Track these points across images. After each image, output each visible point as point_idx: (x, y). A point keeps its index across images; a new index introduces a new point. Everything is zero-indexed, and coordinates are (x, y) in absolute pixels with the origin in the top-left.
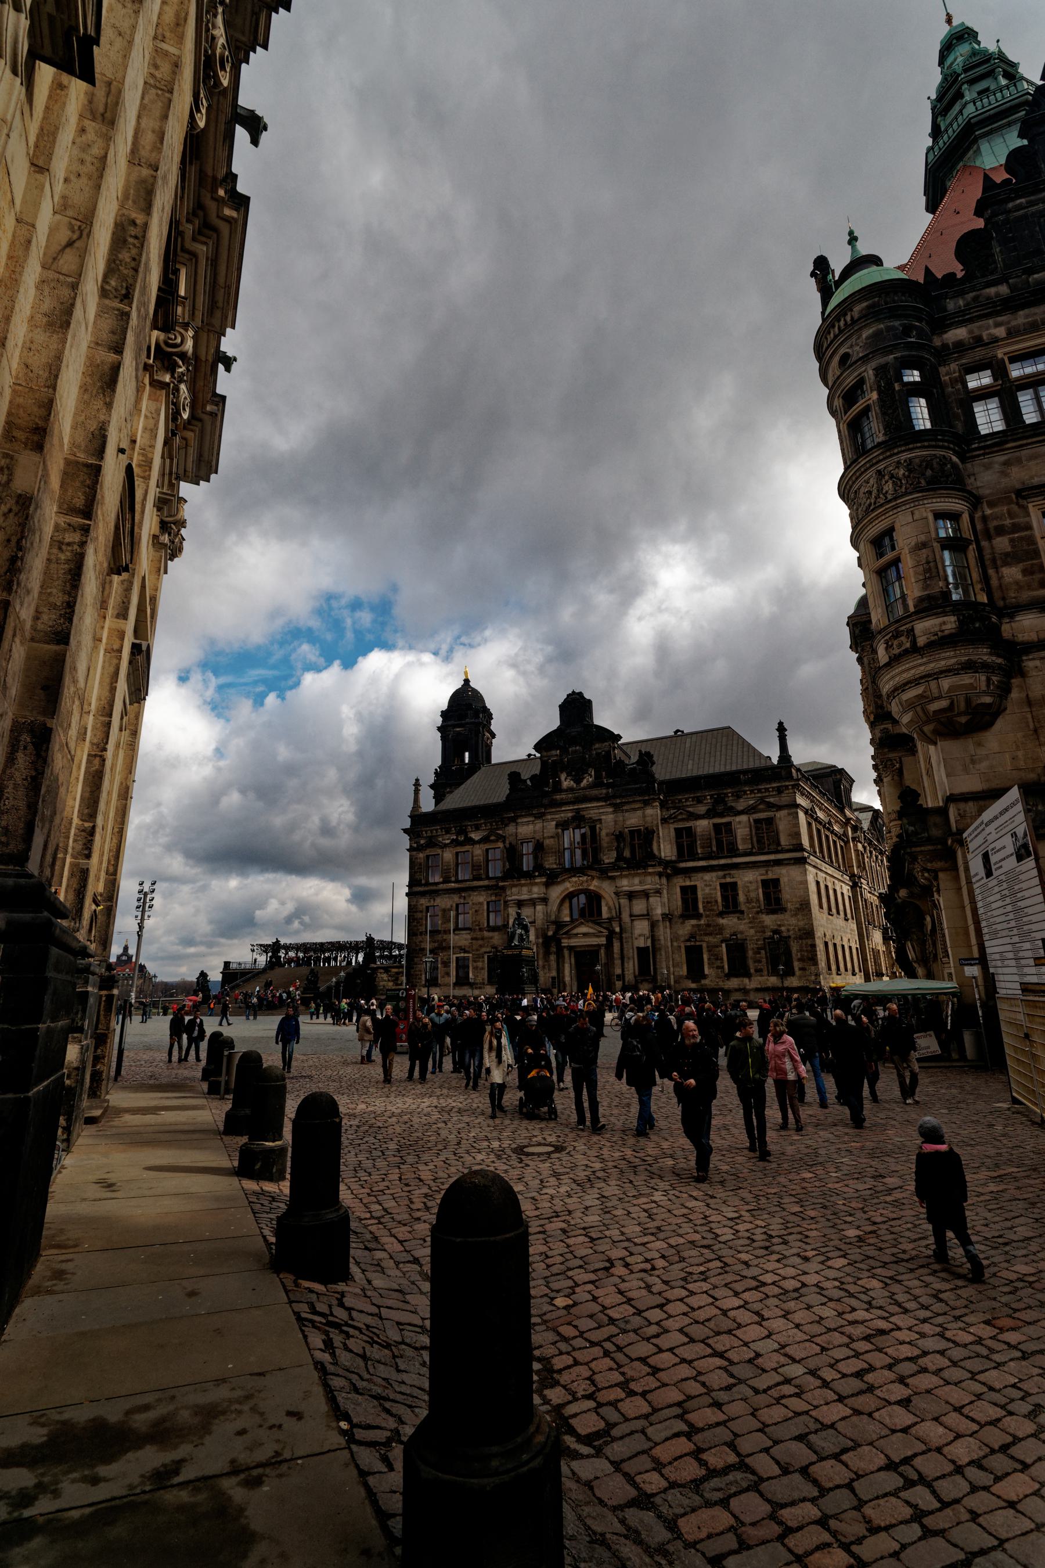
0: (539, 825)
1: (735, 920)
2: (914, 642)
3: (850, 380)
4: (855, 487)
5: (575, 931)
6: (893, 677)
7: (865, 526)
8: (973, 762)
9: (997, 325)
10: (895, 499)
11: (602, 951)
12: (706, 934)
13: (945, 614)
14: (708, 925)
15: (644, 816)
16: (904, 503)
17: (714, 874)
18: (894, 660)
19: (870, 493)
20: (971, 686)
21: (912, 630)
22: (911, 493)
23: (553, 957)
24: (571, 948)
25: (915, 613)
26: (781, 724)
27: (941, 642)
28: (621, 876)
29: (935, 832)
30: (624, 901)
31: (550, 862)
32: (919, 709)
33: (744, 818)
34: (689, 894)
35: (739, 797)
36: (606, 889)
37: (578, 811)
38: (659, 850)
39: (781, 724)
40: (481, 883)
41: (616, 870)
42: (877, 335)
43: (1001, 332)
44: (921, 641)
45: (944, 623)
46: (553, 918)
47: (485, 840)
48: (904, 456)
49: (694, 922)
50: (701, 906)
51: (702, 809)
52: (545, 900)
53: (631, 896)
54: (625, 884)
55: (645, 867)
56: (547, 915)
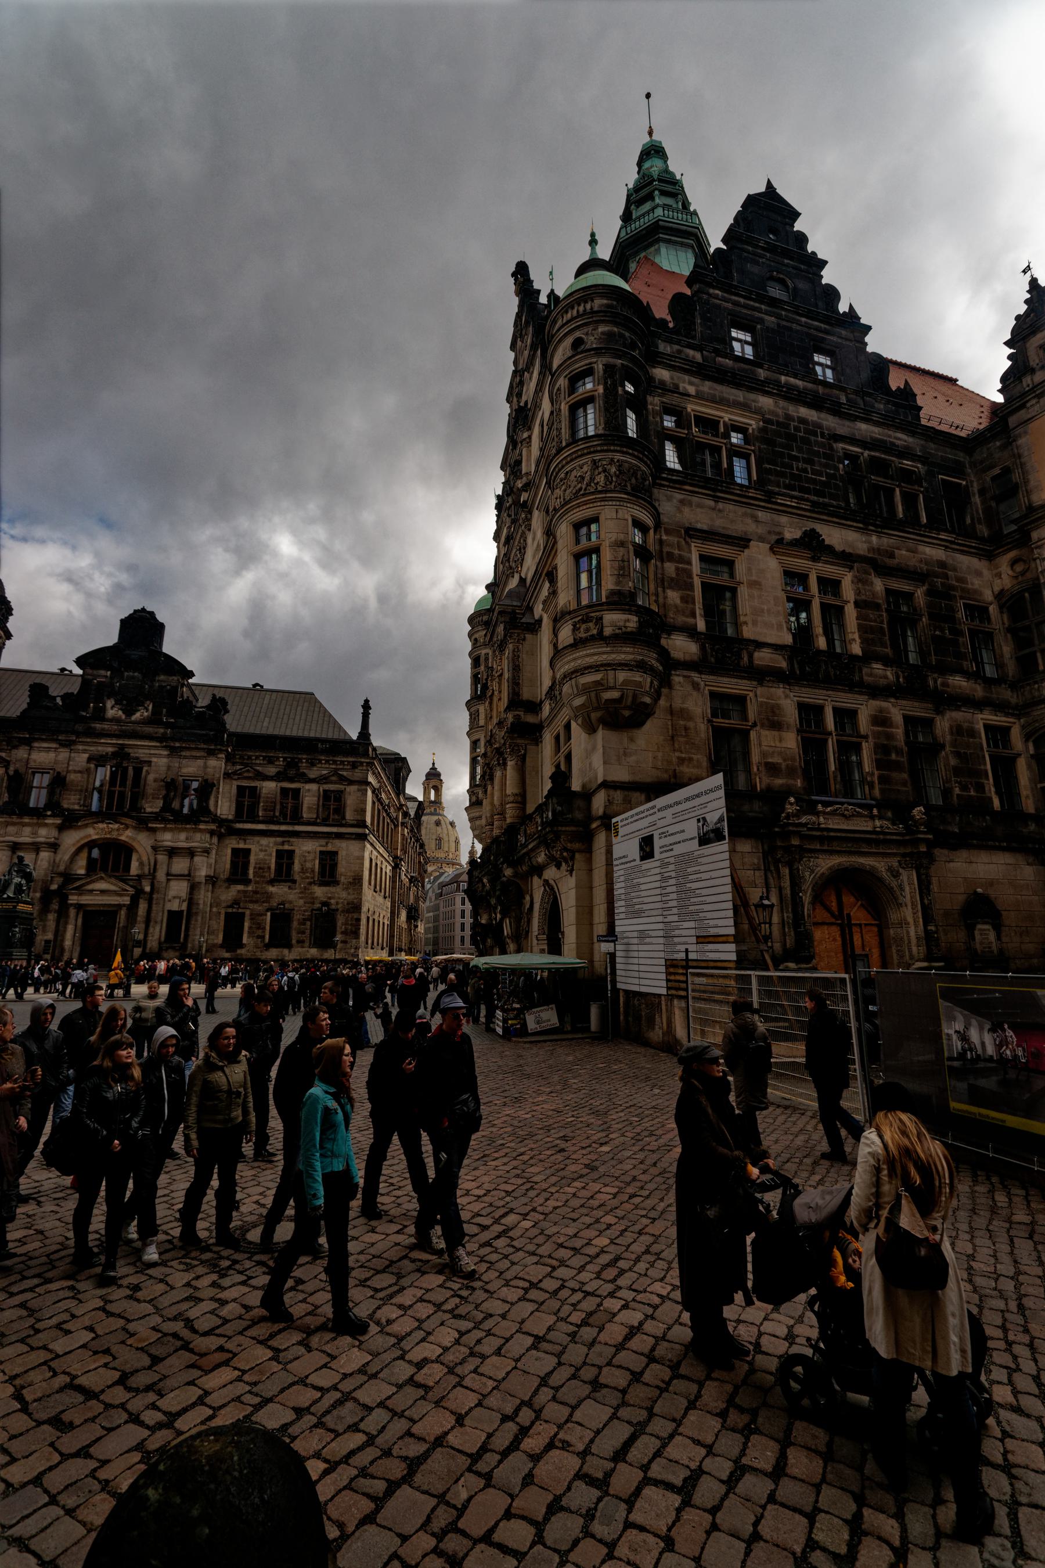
0: (64, 754)
1: (286, 889)
2: (601, 631)
3: (580, 365)
4: (568, 468)
5: (90, 887)
6: (575, 659)
7: (572, 508)
8: (625, 754)
9: (691, 383)
10: (606, 492)
11: (123, 912)
12: (252, 902)
13: (629, 612)
14: (256, 892)
16: (612, 499)
17: (272, 840)
18: (577, 644)
19: (583, 478)
20: (639, 684)
21: (601, 618)
22: (620, 492)
23: (51, 917)
24: (79, 907)
25: (607, 603)
26: (367, 701)
27: (622, 637)
28: (165, 829)
29: (579, 815)
30: (162, 858)
31: (71, 802)
32: (593, 694)
33: (314, 787)
34: (241, 857)
35: (313, 765)
36: (142, 842)
37: (122, 747)
38: (216, 806)
39: (367, 701)
41: (161, 822)
42: (610, 335)
43: (692, 390)
44: (608, 631)
45: (628, 620)
46: (62, 868)
48: (618, 457)
49: (240, 887)
50: (251, 872)
51: (272, 770)
52: (54, 847)
53: (172, 852)
54: (167, 838)
55: (197, 822)
56: (54, 864)
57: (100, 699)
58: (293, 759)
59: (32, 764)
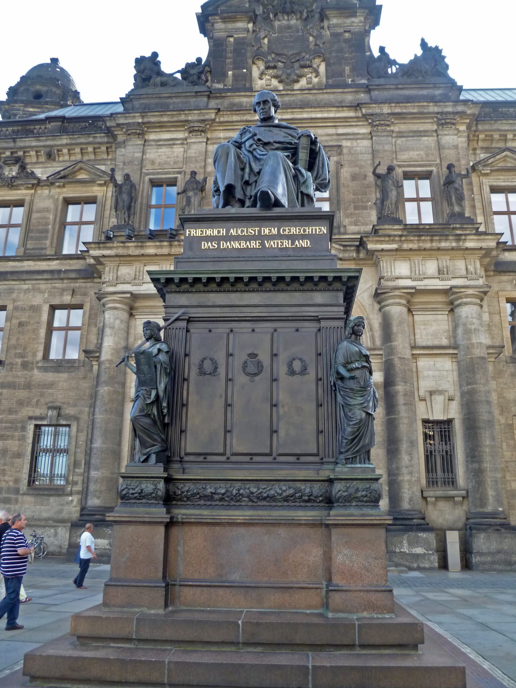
15: (440, 147)
40: (43, 265)
47: (63, 178)
57: (240, 64)
59: (148, 168)
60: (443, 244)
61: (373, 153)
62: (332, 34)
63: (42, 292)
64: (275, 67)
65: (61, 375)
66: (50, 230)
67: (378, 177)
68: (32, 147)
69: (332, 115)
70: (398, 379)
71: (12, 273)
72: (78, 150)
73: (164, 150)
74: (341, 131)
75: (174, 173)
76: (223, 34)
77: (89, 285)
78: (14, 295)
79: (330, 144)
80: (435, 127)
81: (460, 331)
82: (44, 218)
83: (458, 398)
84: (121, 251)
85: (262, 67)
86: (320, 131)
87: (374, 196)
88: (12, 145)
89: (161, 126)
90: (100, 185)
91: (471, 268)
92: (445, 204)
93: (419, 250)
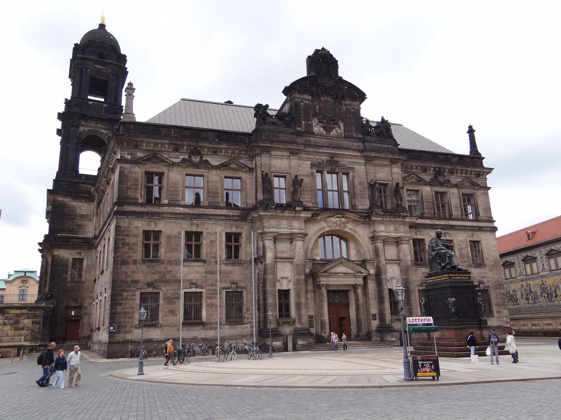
0: (294, 161)
26: (470, 127)
33: (455, 191)
35: (452, 173)
39: (470, 127)
47: (224, 166)
51: (427, 177)
53: (386, 241)
58: (440, 169)
60: (398, 219)
61: (366, 172)
62: (346, 109)
63: (221, 226)
64: (323, 122)
65: (235, 267)
66: (220, 193)
67: (371, 185)
68: (206, 147)
69: (351, 154)
70: (383, 273)
71: (205, 215)
72: (230, 151)
73: (279, 161)
74: (353, 160)
75: (285, 173)
76: (299, 100)
77: (244, 223)
78: (206, 226)
79: (349, 166)
80: (390, 164)
81: (402, 254)
82: (215, 186)
83: (400, 280)
84: (273, 214)
85: (317, 121)
86: (345, 160)
87: (367, 193)
88: (195, 144)
89: (278, 149)
90: (244, 172)
91: (406, 229)
92: (395, 200)
93: (390, 221)
